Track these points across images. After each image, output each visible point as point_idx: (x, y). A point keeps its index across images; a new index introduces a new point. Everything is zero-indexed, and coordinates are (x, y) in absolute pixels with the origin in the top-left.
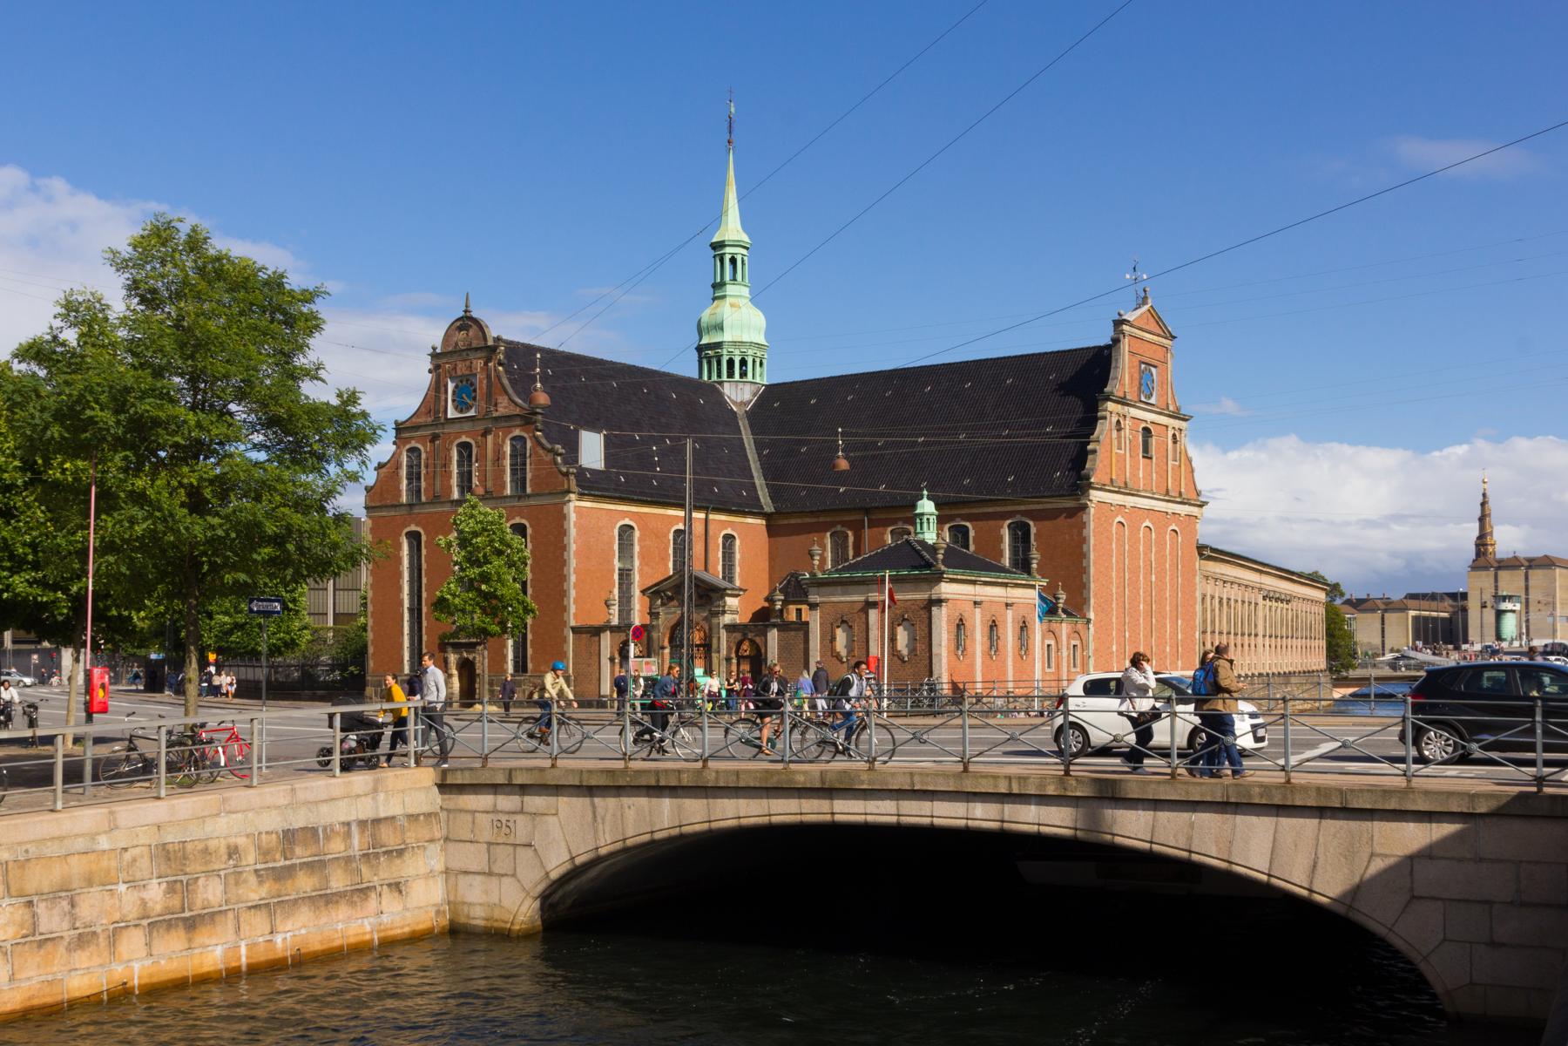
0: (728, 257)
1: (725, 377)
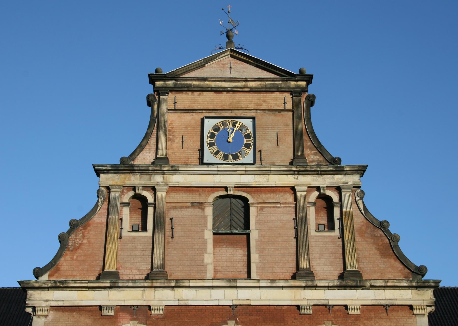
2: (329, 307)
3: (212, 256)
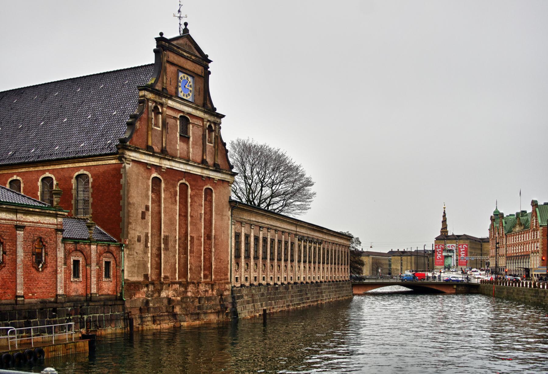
2: (209, 178)
3: (180, 146)
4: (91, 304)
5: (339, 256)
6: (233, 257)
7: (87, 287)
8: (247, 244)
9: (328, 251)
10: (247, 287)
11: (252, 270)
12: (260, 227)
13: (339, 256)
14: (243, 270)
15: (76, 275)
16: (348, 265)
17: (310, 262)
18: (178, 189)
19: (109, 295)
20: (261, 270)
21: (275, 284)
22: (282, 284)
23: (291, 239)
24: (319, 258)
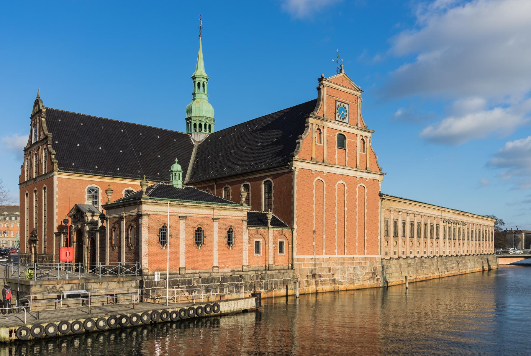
0: (197, 83)
1: (193, 131)
4: (268, 272)
5: (483, 234)
6: (383, 236)
7: (266, 260)
8: (396, 226)
9: (472, 231)
10: (396, 259)
11: (400, 246)
12: (407, 213)
13: (483, 234)
14: (392, 246)
15: (257, 251)
16: (492, 241)
17: (454, 239)
18: (336, 187)
19: (282, 265)
20: (408, 246)
21: (421, 257)
22: (428, 257)
23: (436, 222)
24: (464, 236)
